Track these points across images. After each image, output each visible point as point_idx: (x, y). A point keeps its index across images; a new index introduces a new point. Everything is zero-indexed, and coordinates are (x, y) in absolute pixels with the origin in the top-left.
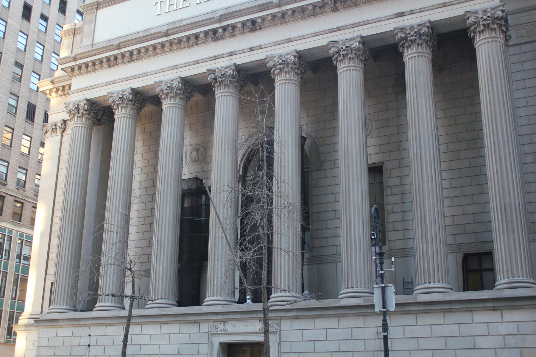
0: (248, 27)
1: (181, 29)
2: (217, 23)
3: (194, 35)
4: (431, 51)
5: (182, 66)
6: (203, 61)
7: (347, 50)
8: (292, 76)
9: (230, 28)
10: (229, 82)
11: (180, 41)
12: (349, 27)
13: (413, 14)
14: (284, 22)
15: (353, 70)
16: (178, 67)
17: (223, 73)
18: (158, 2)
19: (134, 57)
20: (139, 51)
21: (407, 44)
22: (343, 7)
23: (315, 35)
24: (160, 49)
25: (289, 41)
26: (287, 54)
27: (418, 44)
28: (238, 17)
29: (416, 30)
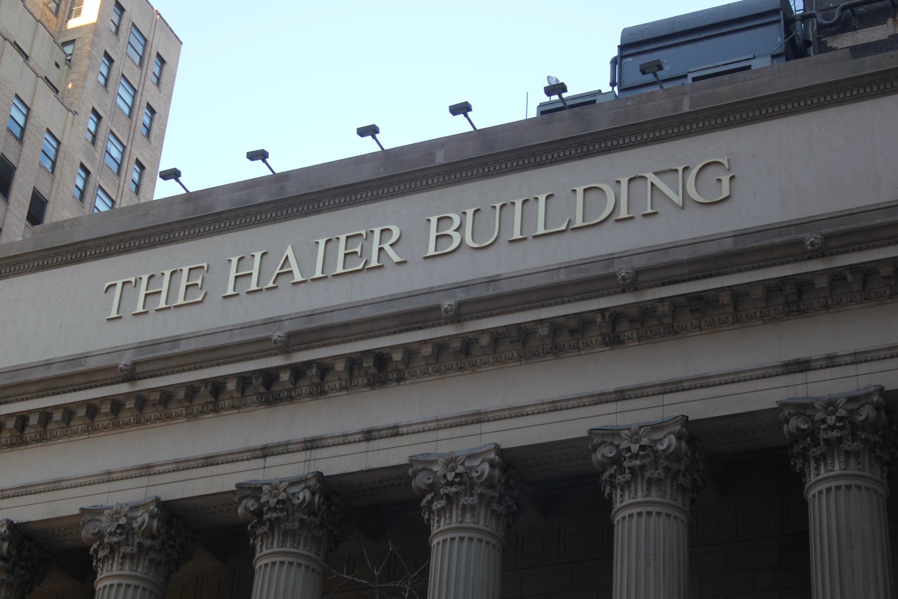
0: (366, 373)
1: (173, 363)
2: (276, 354)
3: (210, 384)
4: (885, 475)
5: (166, 467)
6: (230, 458)
7: (644, 457)
8: (481, 521)
9: (314, 371)
10: (297, 525)
11: (166, 396)
12: (650, 391)
13: (834, 366)
14: (466, 364)
15: (659, 514)
16: (156, 469)
17: (283, 496)
18: (115, 285)
19: (29, 433)
20: (46, 415)
21: (815, 451)
22: (635, 335)
23: (555, 406)
24: (106, 414)
25: (478, 418)
26: (471, 457)
27: (848, 454)
28: (337, 343)
29: (841, 412)
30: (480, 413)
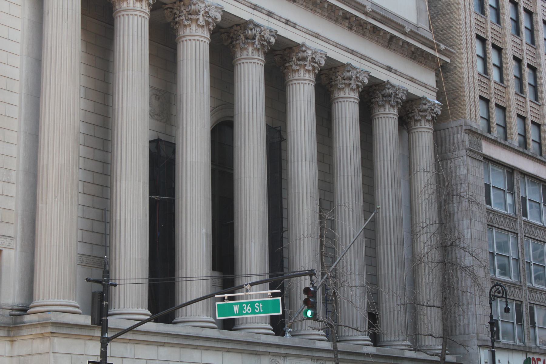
23: (336, 45)
25: (317, 36)
30: (318, 35)
